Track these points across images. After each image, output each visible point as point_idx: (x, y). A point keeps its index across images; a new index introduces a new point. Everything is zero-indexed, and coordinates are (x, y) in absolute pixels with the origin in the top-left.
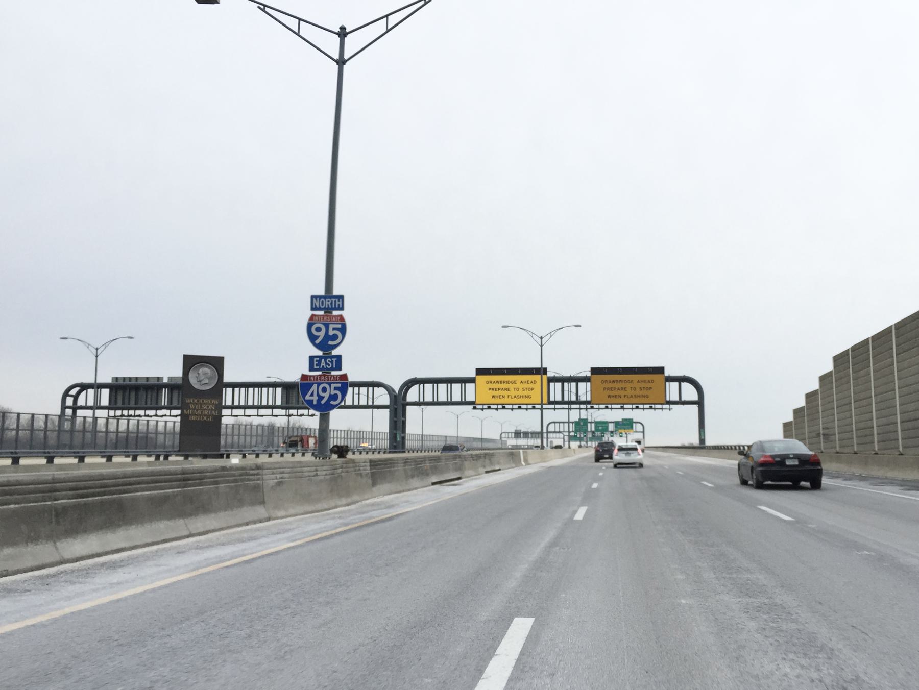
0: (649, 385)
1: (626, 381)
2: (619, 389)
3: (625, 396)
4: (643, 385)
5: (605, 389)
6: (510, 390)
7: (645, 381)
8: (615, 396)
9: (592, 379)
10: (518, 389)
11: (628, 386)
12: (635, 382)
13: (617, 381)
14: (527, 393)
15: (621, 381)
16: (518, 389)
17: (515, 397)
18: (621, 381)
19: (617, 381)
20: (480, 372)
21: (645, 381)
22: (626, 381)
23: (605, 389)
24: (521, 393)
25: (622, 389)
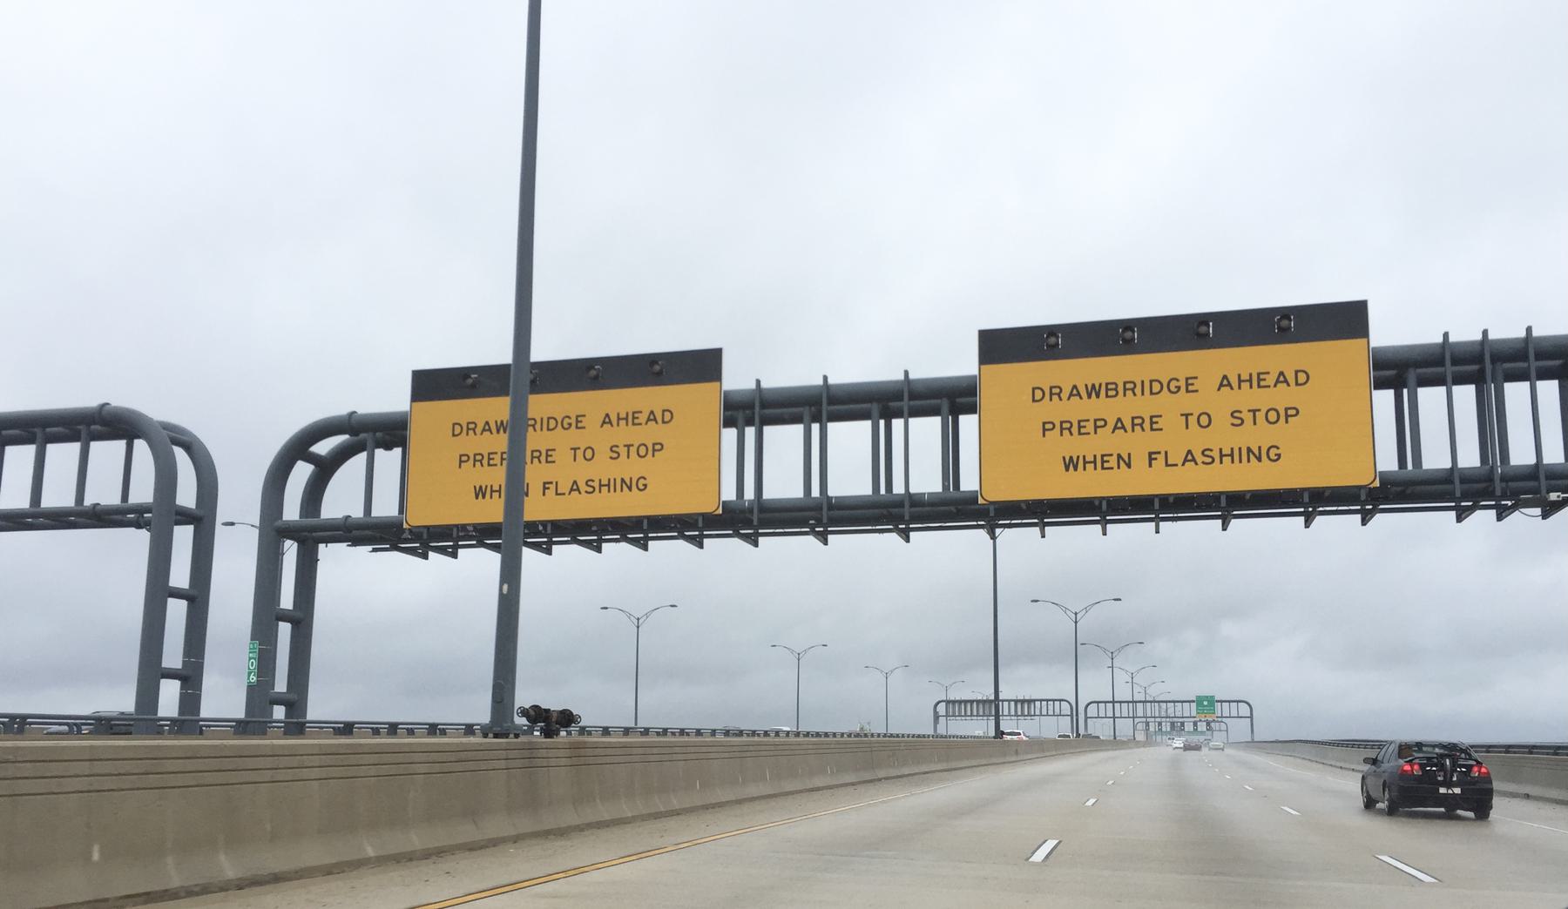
0: (1281, 397)
1: (1154, 387)
2: (1119, 425)
3: (1151, 457)
4: (1247, 398)
5: (1046, 428)
6: (555, 456)
7: (1258, 380)
8: (1101, 462)
9: (985, 397)
10: (589, 454)
11: (1168, 406)
12: (1207, 383)
13: (1111, 389)
14: (630, 468)
15: (1130, 387)
16: (589, 454)
17: (575, 487)
18: (1130, 387)
19: (1111, 389)
20: (429, 385)
21: (1258, 380)
22: (1154, 387)
23: (1046, 428)
24: (603, 469)
25: (1138, 423)
